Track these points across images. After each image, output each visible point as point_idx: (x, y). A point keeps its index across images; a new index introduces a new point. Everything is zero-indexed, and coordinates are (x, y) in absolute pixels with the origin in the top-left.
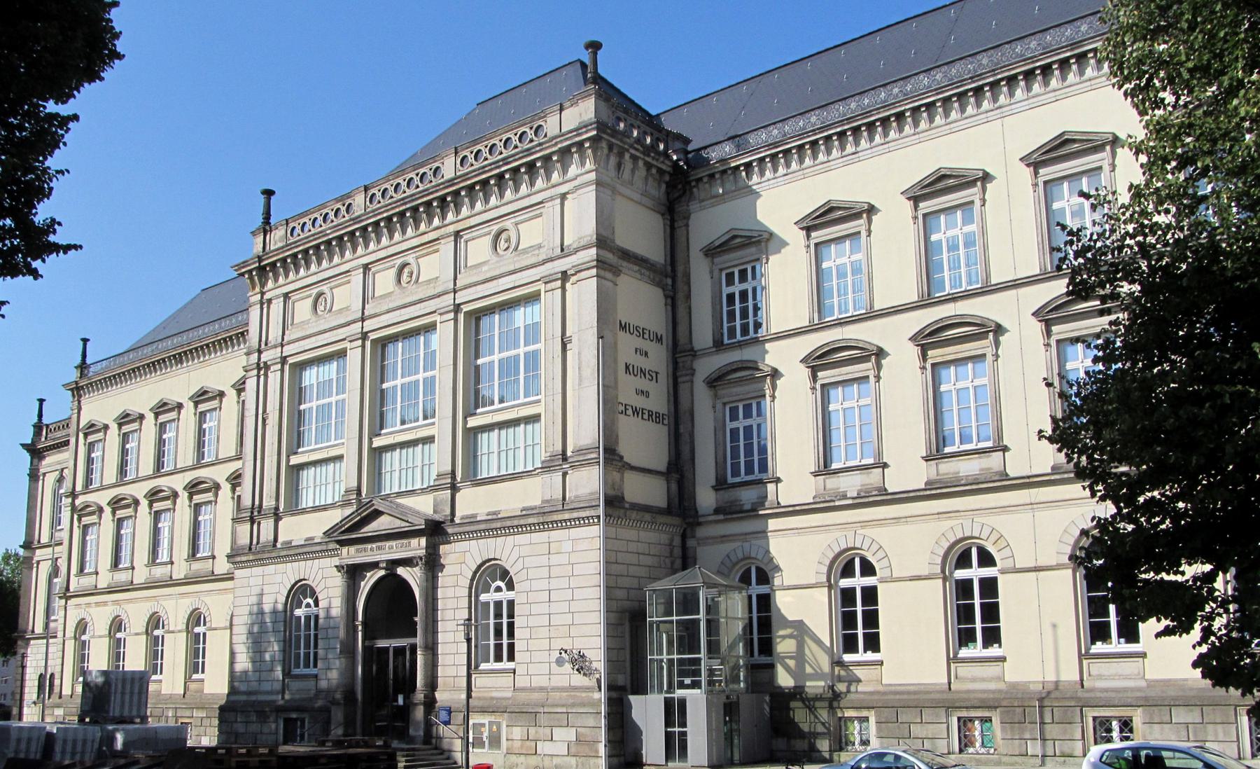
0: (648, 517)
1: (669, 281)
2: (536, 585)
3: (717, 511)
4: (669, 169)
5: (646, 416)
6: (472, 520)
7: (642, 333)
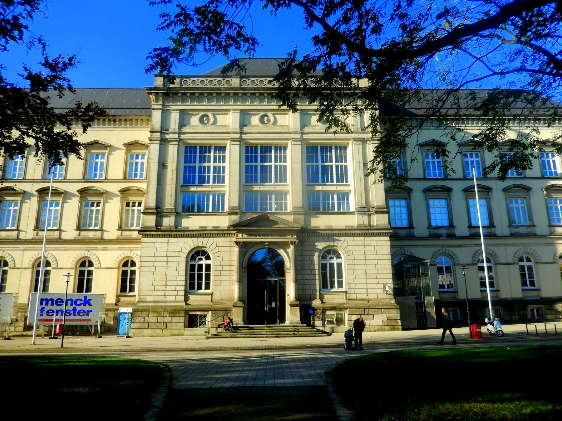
6: (205, 229)
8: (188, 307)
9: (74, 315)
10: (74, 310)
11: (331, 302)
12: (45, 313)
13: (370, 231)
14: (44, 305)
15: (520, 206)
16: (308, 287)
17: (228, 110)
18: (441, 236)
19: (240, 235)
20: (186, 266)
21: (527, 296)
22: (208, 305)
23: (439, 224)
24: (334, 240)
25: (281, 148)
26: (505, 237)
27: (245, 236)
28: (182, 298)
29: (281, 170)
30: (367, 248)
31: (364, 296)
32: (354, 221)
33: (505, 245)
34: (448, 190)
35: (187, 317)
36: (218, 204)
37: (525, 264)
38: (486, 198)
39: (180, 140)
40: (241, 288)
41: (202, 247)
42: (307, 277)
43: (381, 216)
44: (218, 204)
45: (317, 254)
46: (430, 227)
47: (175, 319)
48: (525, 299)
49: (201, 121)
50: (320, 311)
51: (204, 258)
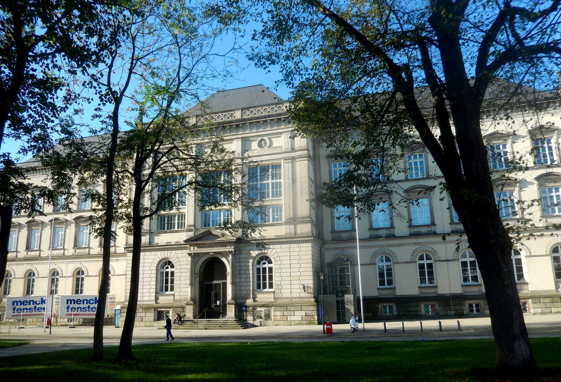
8: (157, 305)
9: (89, 311)
10: (89, 307)
11: (262, 300)
12: (70, 309)
13: (294, 239)
16: (243, 288)
17: (281, 133)
18: (381, 237)
19: (192, 248)
20: (157, 274)
21: (468, 292)
22: (171, 303)
23: (381, 225)
24: (265, 249)
25: (277, 167)
27: (196, 248)
28: (154, 298)
29: (277, 186)
30: (292, 254)
31: (288, 295)
32: (281, 231)
35: (156, 312)
36: (182, 223)
37: (425, 262)
40: (193, 290)
41: (167, 258)
42: (244, 280)
43: (305, 225)
44: (182, 223)
45: (251, 261)
47: (148, 314)
48: (464, 294)
49: (260, 145)
50: (251, 308)
51: (169, 267)
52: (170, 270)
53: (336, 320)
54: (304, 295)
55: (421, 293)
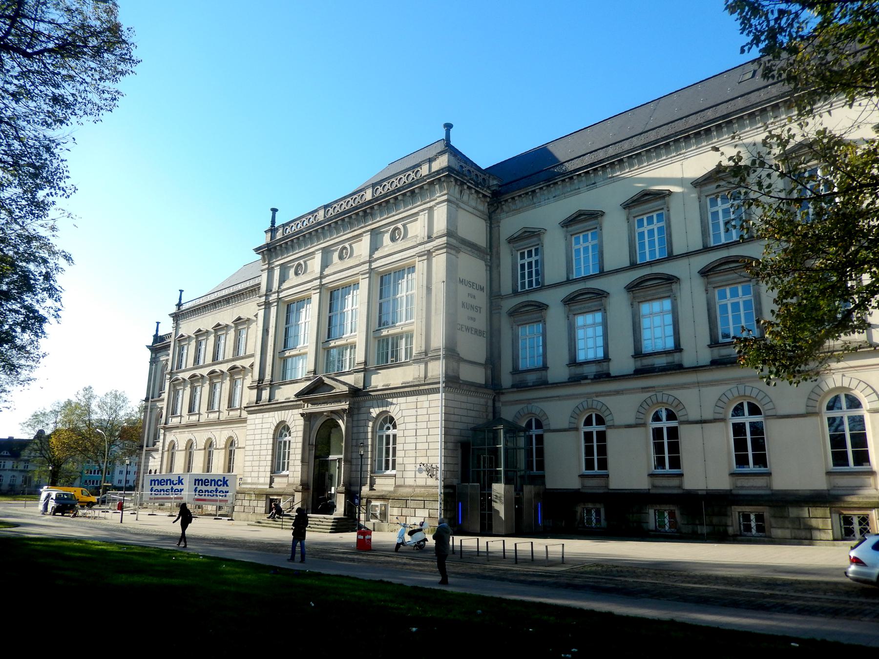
0: (473, 389)
1: (489, 257)
2: (409, 426)
3: (513, 386)
4: (489, 195)
5: (473, 332)
7: (472, 285)
8: (271, 490)
14: (153, 486)
15: (741, 299)
18: (586, 378)
26: (696, 369)
28: (268, 480)
33: (699, 384)
34: (601, 295)
38: (669, 296)
39: (279, 299)
45: (371, 424)
46: (573, 362)
52: (391, 432)
53: (478, 529)
54: (431, 482)
55: (654, 486)
